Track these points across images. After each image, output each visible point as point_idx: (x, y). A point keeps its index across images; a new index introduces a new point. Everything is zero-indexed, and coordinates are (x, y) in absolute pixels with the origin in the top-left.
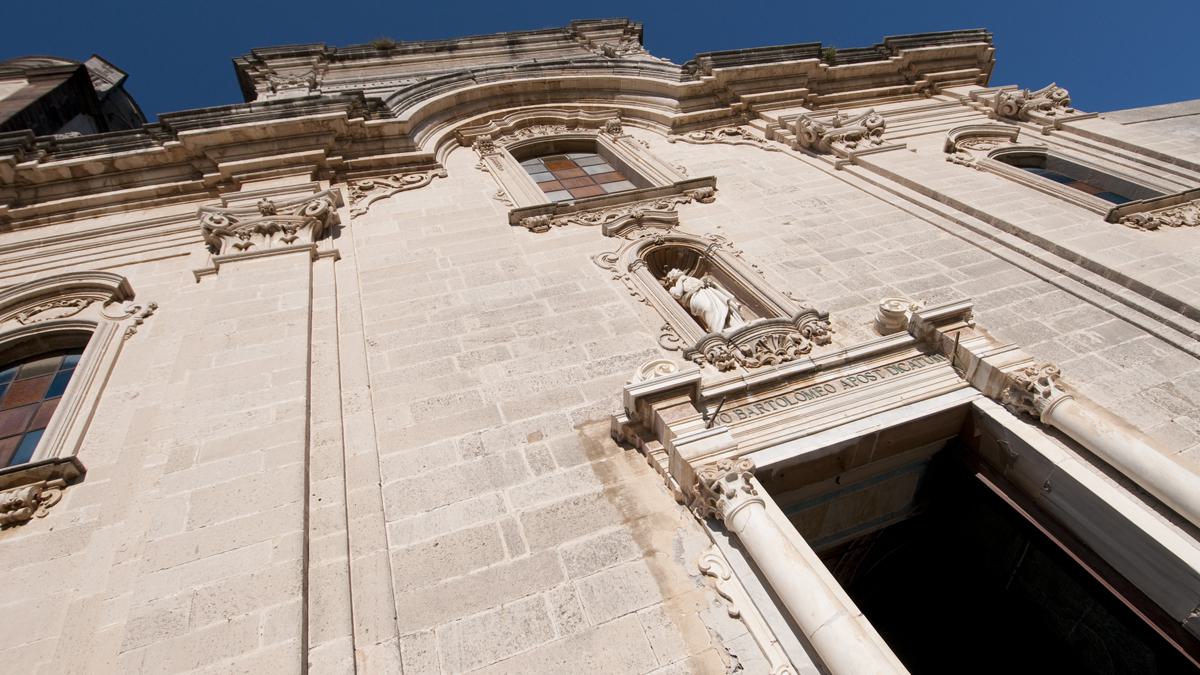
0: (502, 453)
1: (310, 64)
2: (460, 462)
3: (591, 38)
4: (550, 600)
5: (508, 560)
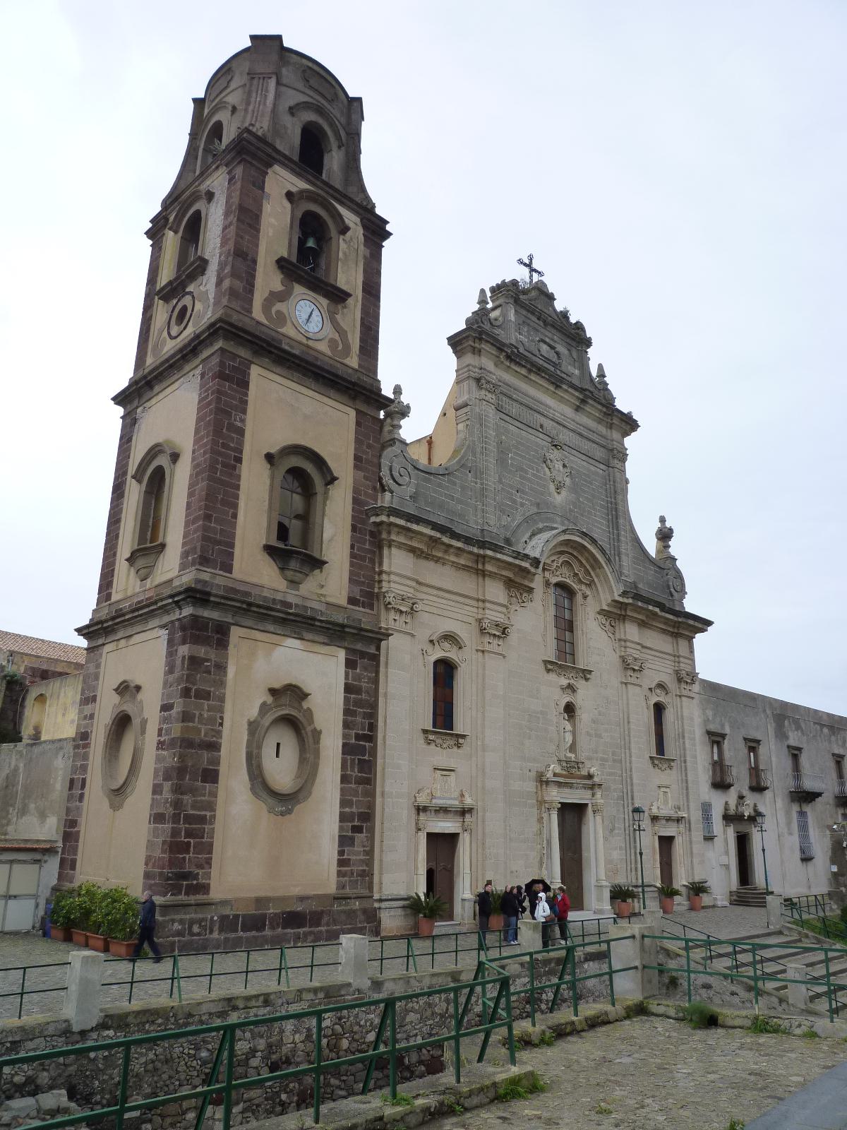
3: (613, 423)
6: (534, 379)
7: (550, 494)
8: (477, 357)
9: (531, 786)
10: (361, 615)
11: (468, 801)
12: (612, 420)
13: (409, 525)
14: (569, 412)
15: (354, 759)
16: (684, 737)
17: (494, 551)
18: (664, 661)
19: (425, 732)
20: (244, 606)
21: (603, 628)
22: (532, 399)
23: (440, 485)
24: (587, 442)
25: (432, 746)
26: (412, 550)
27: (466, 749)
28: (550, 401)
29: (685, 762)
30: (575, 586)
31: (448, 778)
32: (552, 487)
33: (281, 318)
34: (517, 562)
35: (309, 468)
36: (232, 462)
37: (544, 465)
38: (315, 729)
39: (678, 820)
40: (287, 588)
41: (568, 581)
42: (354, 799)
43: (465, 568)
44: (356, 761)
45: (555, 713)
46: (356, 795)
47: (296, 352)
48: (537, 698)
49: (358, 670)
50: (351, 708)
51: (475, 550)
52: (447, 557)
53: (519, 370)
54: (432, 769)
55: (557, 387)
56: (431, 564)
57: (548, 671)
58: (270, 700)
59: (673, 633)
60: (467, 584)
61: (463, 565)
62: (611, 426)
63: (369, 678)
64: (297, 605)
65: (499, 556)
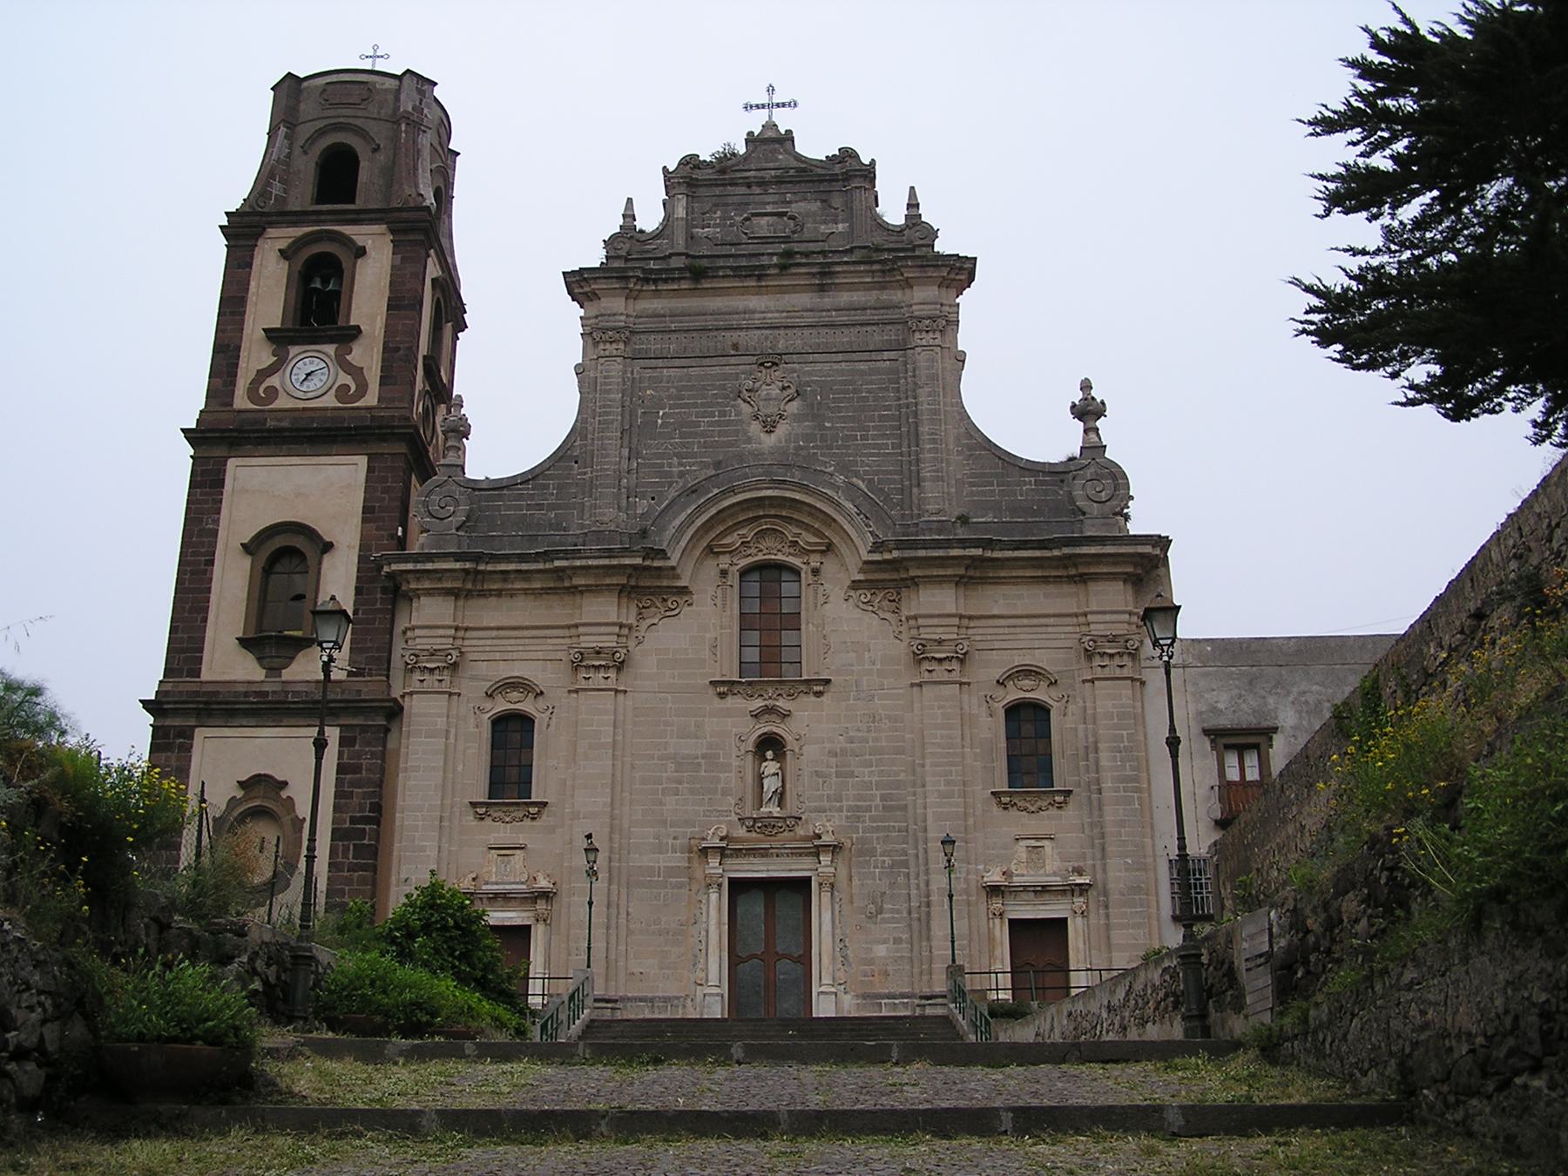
0: (664, 841)
1: (627, 288)
2: (652, 840)
3: (908, 278)
4: (663, 892)
5: (656, 879)
6: (709, 286)
7: (749, 440)
8: (595, 302)
9: (678, 859)
10: (369, 688)
11: (543, 883)
12: (902, 275)
13: (420, 566)
14: (804, 299)
15: (349, 845)
16: (1096, 750)
17: (567, 559)
18: (1050, 629)
19: (474, 805)
20: (201, 706)
21: (871, 608)
22: (711, 314)
23: (520, 498)
24: (846, 331)
25: (488, 821)
26: (448, 592)
27: (546, 819)
28: (754, 302)
29: (1100, 791)
30: (796, 561)
31: (511, 858)
32: (755, 428)
33: (273, 393)
34: (615, 562)
35: (299, 542)
36: (202, 567)
37: (739, 401)
38: (297, 817)
39: (1083, 889)
40: (266, 677)
41: (780, 557)
42: (347, 888)
43: (546, 591)
44: (351, 847)
45: (735, 752)
46: (349, 881)
47: (285, 424)
48: (697, 738)
49: (357, 747)
50: (346, 789)
51: (541, 566)
52: (510, 586)
53: (676, 287)
54: (486, 849)
55: (760, 278)
56: (493, 601)
57: (722, 695)
58: (239, 794)
59: (1068, 577)
60: (557, 611)
61: (542, 589)
62: (908, 284)
63: (373, 753)
64: (274, 692)
65: (578, 563)
